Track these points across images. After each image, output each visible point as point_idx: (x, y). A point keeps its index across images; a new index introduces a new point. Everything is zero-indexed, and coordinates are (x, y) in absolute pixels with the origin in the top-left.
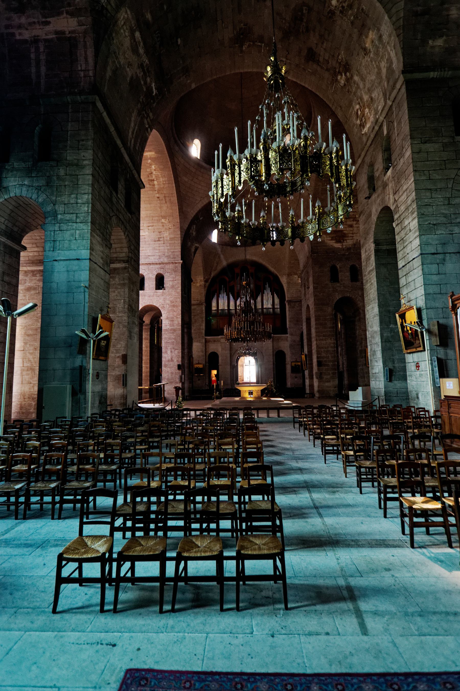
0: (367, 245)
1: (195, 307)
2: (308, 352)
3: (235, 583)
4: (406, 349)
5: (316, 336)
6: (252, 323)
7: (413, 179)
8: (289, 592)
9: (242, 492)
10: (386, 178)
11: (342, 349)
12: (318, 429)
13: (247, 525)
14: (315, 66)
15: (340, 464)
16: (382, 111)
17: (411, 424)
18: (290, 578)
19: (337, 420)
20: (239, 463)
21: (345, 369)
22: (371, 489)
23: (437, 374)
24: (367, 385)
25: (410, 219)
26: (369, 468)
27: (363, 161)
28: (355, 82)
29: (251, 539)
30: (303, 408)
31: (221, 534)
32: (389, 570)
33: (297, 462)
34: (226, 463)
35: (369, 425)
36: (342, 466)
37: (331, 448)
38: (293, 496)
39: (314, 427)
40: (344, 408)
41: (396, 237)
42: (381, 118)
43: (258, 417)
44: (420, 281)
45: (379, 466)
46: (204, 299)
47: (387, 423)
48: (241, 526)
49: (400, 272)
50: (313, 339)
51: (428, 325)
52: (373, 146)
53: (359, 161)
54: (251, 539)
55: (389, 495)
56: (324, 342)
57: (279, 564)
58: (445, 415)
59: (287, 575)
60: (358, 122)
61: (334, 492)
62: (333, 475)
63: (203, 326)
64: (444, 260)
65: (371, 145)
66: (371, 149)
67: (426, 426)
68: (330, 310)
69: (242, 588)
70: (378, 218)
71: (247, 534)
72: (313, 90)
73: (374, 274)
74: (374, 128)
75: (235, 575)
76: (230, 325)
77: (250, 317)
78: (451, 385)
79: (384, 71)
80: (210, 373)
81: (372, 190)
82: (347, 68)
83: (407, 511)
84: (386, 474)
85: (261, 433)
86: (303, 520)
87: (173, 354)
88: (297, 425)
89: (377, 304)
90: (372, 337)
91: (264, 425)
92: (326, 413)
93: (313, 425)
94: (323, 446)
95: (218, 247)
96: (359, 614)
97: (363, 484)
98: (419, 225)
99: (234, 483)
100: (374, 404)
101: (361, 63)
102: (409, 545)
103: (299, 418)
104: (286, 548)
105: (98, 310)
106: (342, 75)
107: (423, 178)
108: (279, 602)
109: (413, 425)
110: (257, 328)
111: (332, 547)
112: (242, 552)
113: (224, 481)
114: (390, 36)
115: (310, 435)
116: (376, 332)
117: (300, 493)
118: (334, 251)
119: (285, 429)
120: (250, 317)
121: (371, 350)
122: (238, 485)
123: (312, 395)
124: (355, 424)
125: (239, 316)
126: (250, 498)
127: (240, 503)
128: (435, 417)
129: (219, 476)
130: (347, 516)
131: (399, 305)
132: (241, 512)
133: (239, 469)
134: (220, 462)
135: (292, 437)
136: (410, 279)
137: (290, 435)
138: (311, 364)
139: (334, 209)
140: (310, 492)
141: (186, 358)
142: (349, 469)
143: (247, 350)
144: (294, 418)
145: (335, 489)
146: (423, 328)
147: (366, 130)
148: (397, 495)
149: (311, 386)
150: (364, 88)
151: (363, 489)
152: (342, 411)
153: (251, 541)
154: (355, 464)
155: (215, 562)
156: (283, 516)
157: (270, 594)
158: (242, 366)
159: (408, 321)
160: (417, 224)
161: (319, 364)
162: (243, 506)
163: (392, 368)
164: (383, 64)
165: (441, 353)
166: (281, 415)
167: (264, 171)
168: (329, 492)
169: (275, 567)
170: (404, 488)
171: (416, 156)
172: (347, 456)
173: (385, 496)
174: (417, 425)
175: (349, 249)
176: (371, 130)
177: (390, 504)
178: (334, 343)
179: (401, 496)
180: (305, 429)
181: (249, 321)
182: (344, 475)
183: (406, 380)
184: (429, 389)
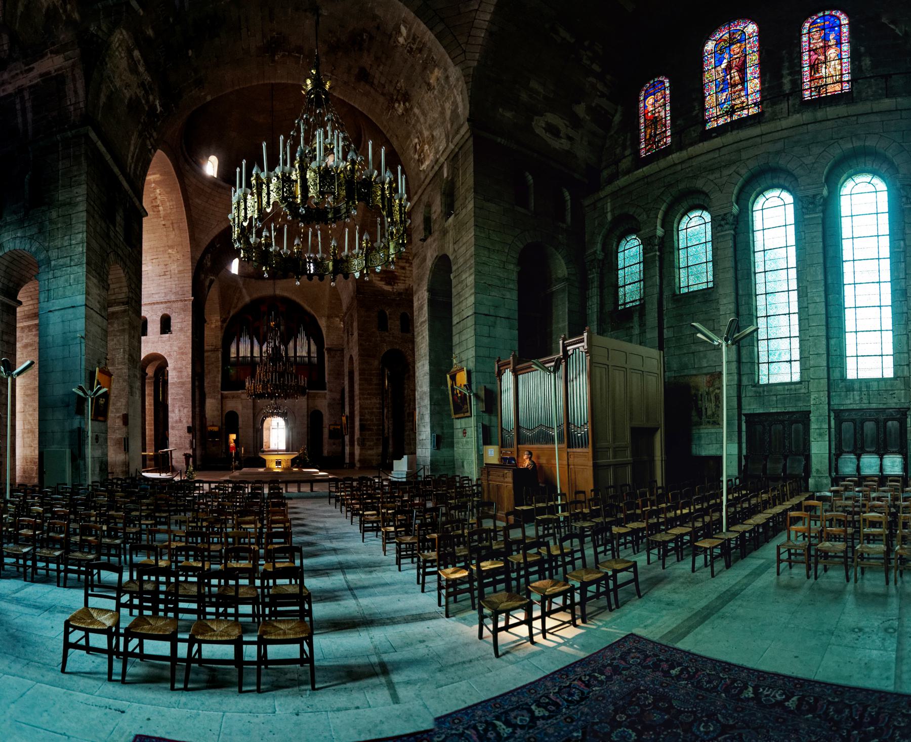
1: (209, 353)
2: (350, 413)
3: (256, 667)
4: (455, 414)
5: (360, 393)
6: (282, 375)
8: (317, 674)
9: (265, 576)
11: (388, 411)
12: (357, 504)
13: (270, 610)
15: (380, 542)
17: (454, 495)
18: (319, 660)
19: (379, 494)
20: (262, 544)
21: (390, 434)
22: (411, 566)
23: (481, 442)
24: (413, 453)
26: (409, 544)
29: (275, 624)
30: (340, 480)
31: (240, 619)
32: (424, 641)
33: (331, 542)
34: (247, 544)
35: (412, 498)
36: (381, 543)
37: (370, 525)
38: (325, 579)
40: (387, 480)
43: (286, 491)
45: (419, 541)
46: (220, 343)
47: (430, 495)
48: (264, 611)
50: (356, 398)
51: (476, 389)
54: (275, 624)
55: (428, 570)
56: (369, 401)
57: (306, 647)
58: (485, 483)
59: (316, 657)
61: (371, 572)
62: (371, 554)
63: (219, 378)
69: (263, 671)
71: (270, 619)
75: (256, 659)
76: (253, 376)
77: (280, 366)
80: (227, 438)
83: (444, 583)
85: (289, 511)
87: (182, 414)
88: (333, 501)
90: (421, 398)
91: (294, 501)
92: (366, 486)
93: (352, 500)
94: (362, 522)
96: (391, 686)
97: (403, 561)
99: (256, 566)
102: (444, 616)
103: (336, 492)
104: (315, 632)
105: (95, 363)
108: (306, 683)
109: (456, 496)
112: (265, 637)
113: (244, 564)
115: (347, 511)
116: (425, 393)
119: (318, 505)
120: (280, 366)
121: (419, 413)
122: (261, 568)
123: (352, 465)
124: (398, 497)
125: (266, 365)
126: (274, 582)
127: (262, 587)
128: (477, 485)
129: (238, 558)
131: (451, 365)
132: (264, 596)
133: (262, 551)
134: (239, 543)
135: (326, 514)
137: (324, 512)
138: (353, 428)
141: (197, 418)
142: (388, 547)
143: (275, 409)
144: (330, 492)
145: (373, 569)
146: (471, 392)
149: (352, 454)
151: (402, 566)
152: (385, 483)
153: (275, 627)
154: (395, 540)
155: (233, 646)
156: (312, 600)
157: (296, 676)
158: (269, 429)
159: (458, 385)
161: (363, 428)
162: (266, 590)
165: (486, 419)
166: (315, 489)
168: (366, 572)
169: (302, 650)
172: (387, 533)
173: (424, 571)
178: (379, 403)
179: (439, 569)
180: (343, 504)
182: (383, 553)
183: (453, 447)
184: (474, 457)
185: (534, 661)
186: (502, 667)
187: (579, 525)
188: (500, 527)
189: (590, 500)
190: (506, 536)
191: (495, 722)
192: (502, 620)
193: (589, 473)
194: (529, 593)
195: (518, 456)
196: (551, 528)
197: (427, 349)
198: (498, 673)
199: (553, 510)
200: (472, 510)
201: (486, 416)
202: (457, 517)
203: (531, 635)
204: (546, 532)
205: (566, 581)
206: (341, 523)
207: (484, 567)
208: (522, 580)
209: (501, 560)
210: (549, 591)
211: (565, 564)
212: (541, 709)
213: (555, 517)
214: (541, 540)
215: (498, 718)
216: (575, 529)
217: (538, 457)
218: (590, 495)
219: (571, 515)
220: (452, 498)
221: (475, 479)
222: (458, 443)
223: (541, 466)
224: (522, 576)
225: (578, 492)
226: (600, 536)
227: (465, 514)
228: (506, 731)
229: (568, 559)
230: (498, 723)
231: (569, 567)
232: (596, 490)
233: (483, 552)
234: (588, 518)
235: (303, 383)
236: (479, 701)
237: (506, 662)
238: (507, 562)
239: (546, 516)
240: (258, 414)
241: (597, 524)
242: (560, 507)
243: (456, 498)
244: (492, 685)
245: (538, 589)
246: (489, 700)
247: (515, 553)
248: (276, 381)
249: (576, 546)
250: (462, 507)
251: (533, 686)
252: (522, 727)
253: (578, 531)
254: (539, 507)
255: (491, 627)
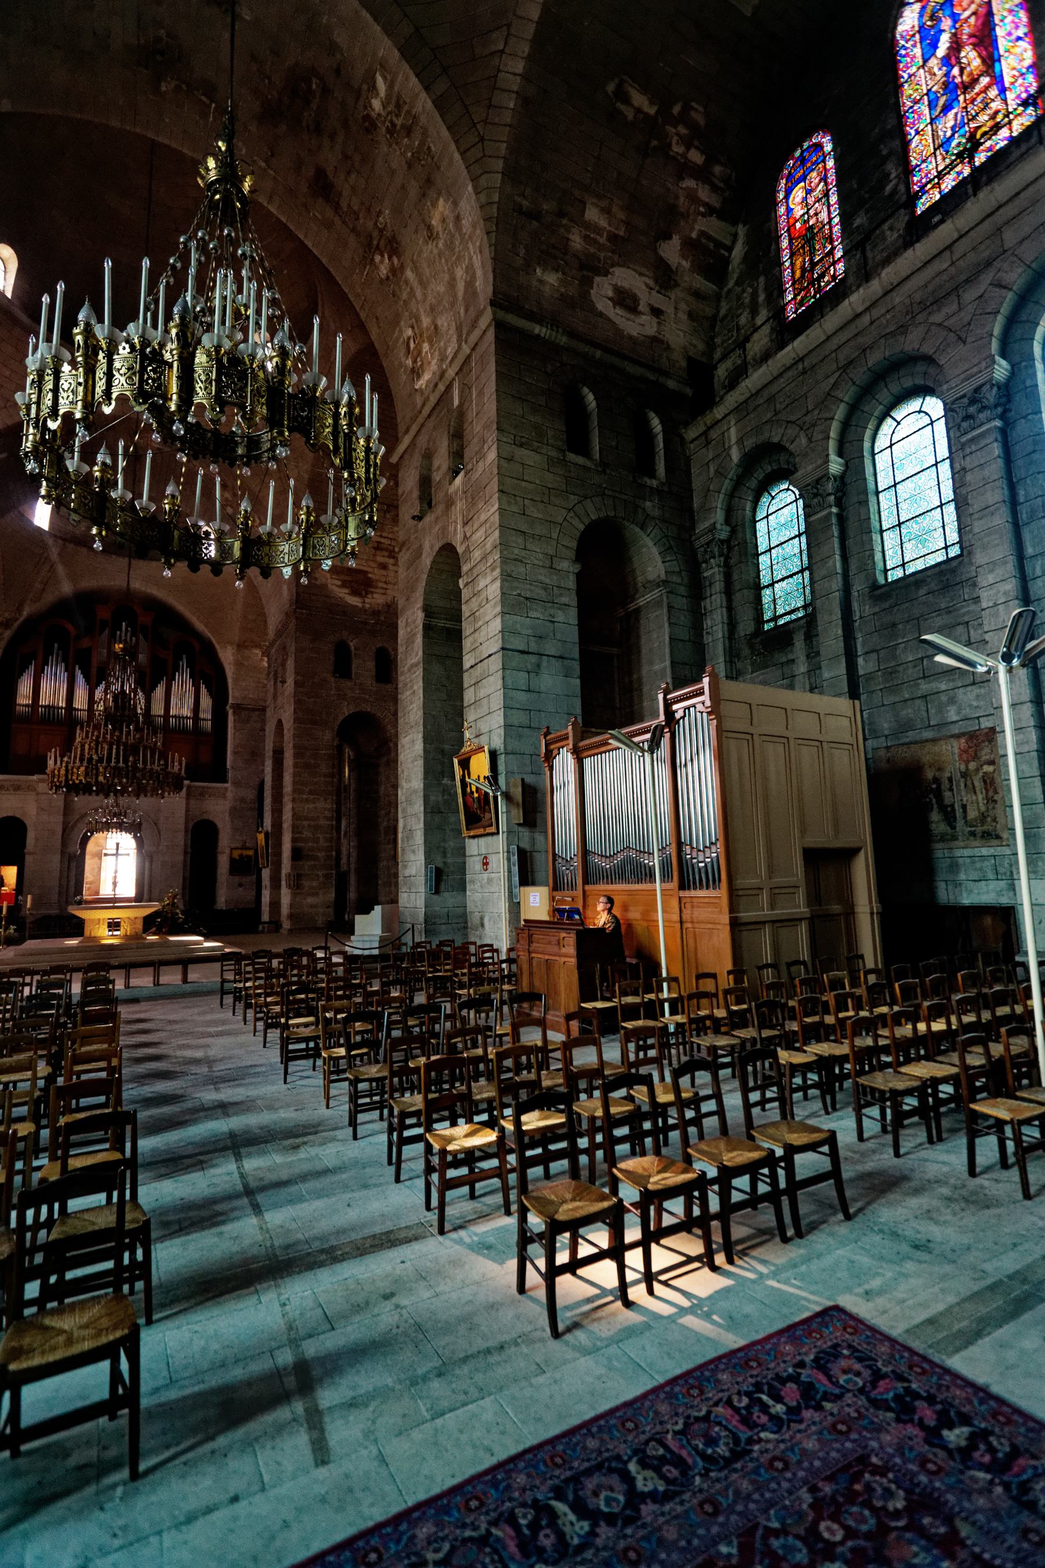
0: (409, 613)
5: (294, 791)
7: (496, 506)
10: (452, 489)
12: (276, 1003)
14: (329, 213)
16: (453, 359)
17: (466, 979)
19: (322, 981)
23: (516, 879)
25: (489, 579)
27: (413, 443)
28: (407, 282)
33: (217, 1089)
36: (321, 1082)
37: (303, 1046)
39: (269, 999)
41: (464, 607)
42: (451, 373)
44: (497, 701)
49: (466, 676)
50: (287, 800)
51: (507, 784)
52: (433, 418)
53: (406, 441)
56: (311, 806)
58: (524, 957)
60: (409, 362)
61: (296, 1147)
64: (539, 666)
65: (429, 416)
66: (430, 424)
67: (491, 981)
68: (327, 736)
70: (433, 562)
72: (324, 261)
73: (419, 672)
74: (436, 385)
78: (538, 900)
79: (461, 286)
81: (426, 506)
82: (393, 248)
84: (407, 1089)
86: (214, 1230)
88: (229, 1000)
89: (421, 736)
90: (409, 801)
93: (267, 995)
94: (285, 1042)
95: (50, 542)
98: (503, 594)
100: (404, 940)
101: (421, 251)
103: (235, 981)
106: (382, 256)
107: (515, 509)
109: (470, 980)
110: (145, 762)
111: (275, 1279)
114: (474, 226)
115: (257, 1020)
116: (415, 791)
117: (213, 1166)
118: (346, 610)
119: (196, 1010)
124: (359, 986)
128: (510, 961)
130: (318, 1198)
136: (482, 693)
139: (340, 522)
140: (238, 1157)
146: (497, 790)
147: (421, 383)
148: (420, 1131)
149: (275, 905)
150: (424, 300)
152: (336, 959)
154: (348, 1075)
159: (474, 776)
160: (499, 591)
163: (440, 865)
164: (459, 272)
166: (191, 977)
167: (174, 389)
170: (437, 1111)
171: (503, 463)
174: (477, 980)
175: (375, 613)
176: (431, 386)
177: (408, 1151)
180: (248, 1006)
181: (125, 745)
182: (324, 1103)
183: (465, 890)
184: (502, 907)
185: (631, 1348)
186: (565, 1362)
187: (706, 1041)
188: (554, 1043)
189: (726, 992)
190: (568, 1061)
191: (553, 1503)
192: (563, 1249)
193: (722, 938)
194: (614, 1184)
195: (584, 906)
196: (652, 1047)
197: (420, 713)
198: (558, 1376)
199: (653, 1010)
200: (500, 1009)
201: (525, 833)
202: (472, 1023)
203: (623, 1285)
204: (641, 1054)
205: (688, 1160)
206: (241, 1046)
207: (526, 1124)
208: (600, 1154)
209: (561, 1111)
210: (657, 1181)
211: (683, 1124)
212: (649, 1473)
213: (660, 1025)
214: (633, 1071)
215: (559, 1495)
216: (699, 1051)
217: (625, 908)
218: (726, 982)
219: (691, 1021)
220: (462, 986)
221: (504, 950)
222: (473, 882)
223: (630, 926)
224: (599, 1146)
225: (700, 976)
226: (750, 1069)
227: (487, 1016)
228: (577, 1528)
229: (690, 1114)
230: (561, 1507)
231: (692, 1130)
232: (738, 972)
233: (523, 1095)
234: (723, 1029)
235: (176, 769)
236: (520, 1448)
237: (574, 1348)
238: (570, 1113)
239: (640, 1023)
240: (73, 827)
241: (744, 1042)
242: (666, 1005)
243: (470, 986)
244: (547, 1407)
245: (634, 1177)
246: (540, 1446)
247: (583, 1096)
248: (118, 761)
249: (704, 1086)
250: (482, 1003)
251: (630, 1412)
252: (610, 1519)
253: (704, 1054)
254: (627, 1005)
255: (541, 1263)
